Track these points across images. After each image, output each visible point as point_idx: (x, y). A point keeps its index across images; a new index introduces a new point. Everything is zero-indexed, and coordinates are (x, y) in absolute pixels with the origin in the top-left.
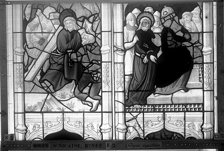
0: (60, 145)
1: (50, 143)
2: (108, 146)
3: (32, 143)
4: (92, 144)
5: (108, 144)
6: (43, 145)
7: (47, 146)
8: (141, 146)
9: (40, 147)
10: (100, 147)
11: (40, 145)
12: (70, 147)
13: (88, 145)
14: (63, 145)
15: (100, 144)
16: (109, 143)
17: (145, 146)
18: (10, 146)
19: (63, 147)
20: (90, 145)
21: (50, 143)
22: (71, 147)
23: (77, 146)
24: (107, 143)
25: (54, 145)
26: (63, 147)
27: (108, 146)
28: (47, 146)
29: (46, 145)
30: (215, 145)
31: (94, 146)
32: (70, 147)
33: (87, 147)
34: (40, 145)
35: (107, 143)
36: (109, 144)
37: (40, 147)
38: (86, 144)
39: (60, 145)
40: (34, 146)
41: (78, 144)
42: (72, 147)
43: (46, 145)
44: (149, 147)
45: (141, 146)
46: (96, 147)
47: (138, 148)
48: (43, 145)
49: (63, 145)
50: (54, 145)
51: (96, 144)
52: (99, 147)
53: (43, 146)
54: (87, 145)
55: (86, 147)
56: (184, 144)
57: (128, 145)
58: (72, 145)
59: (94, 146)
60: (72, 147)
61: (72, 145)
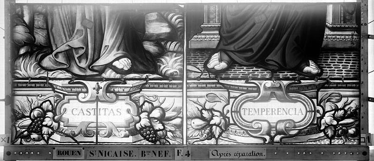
0: (100, 151)
1: (83, 149)
2: (178, 155)
3: (54, 149)
4: (153, 151)
5: (178, 150)
6: (73, 151)
7: (80, 154)
8: (232, 154)
9: (68, 154)
10: (165, 156)
11: (68, 151)
12: (117, 156)
13: (146, 152)
14: (105, 152)
15: (165, 152)
16: (181, 149)
17: (238, 155)
18: (20, 154)
19: (105, 156)
20: (150, 152)
21: (83, 149)
22: (118, 154)
23: (127, 154)
24: (176, 150)
25: (93, 154)
26: (105, 156)
27: (178, 155)
28: (80, 154)
29: (78, 152)
30: (353, 154)
31: (155, 155)
32: (117, 156)
33: (145, 155)
34: (68, 151)
35: (176, 150)
36: (180, 151)
37: (68, 154)
38: (142, 152)
39: (100, 151)
40: (59, 154)
41: (130, 151)
42: (121, 156)
43: (78, 152)
44: (244, 157)
45: (232, 154)
46: (159, 156)
47: (227, 157)
48: (73, 151)
49: (105, 152)
50: (93, 154)
51: (159, 152)
52: (164, 155)
53: (73, 154)
54: (145, 152)
55: (142, 156)
56: (301, 152)
57: (210, 152)
58: (121, 152)
59: (155, 155)
60: (121, 156)
61: (121, 152)
